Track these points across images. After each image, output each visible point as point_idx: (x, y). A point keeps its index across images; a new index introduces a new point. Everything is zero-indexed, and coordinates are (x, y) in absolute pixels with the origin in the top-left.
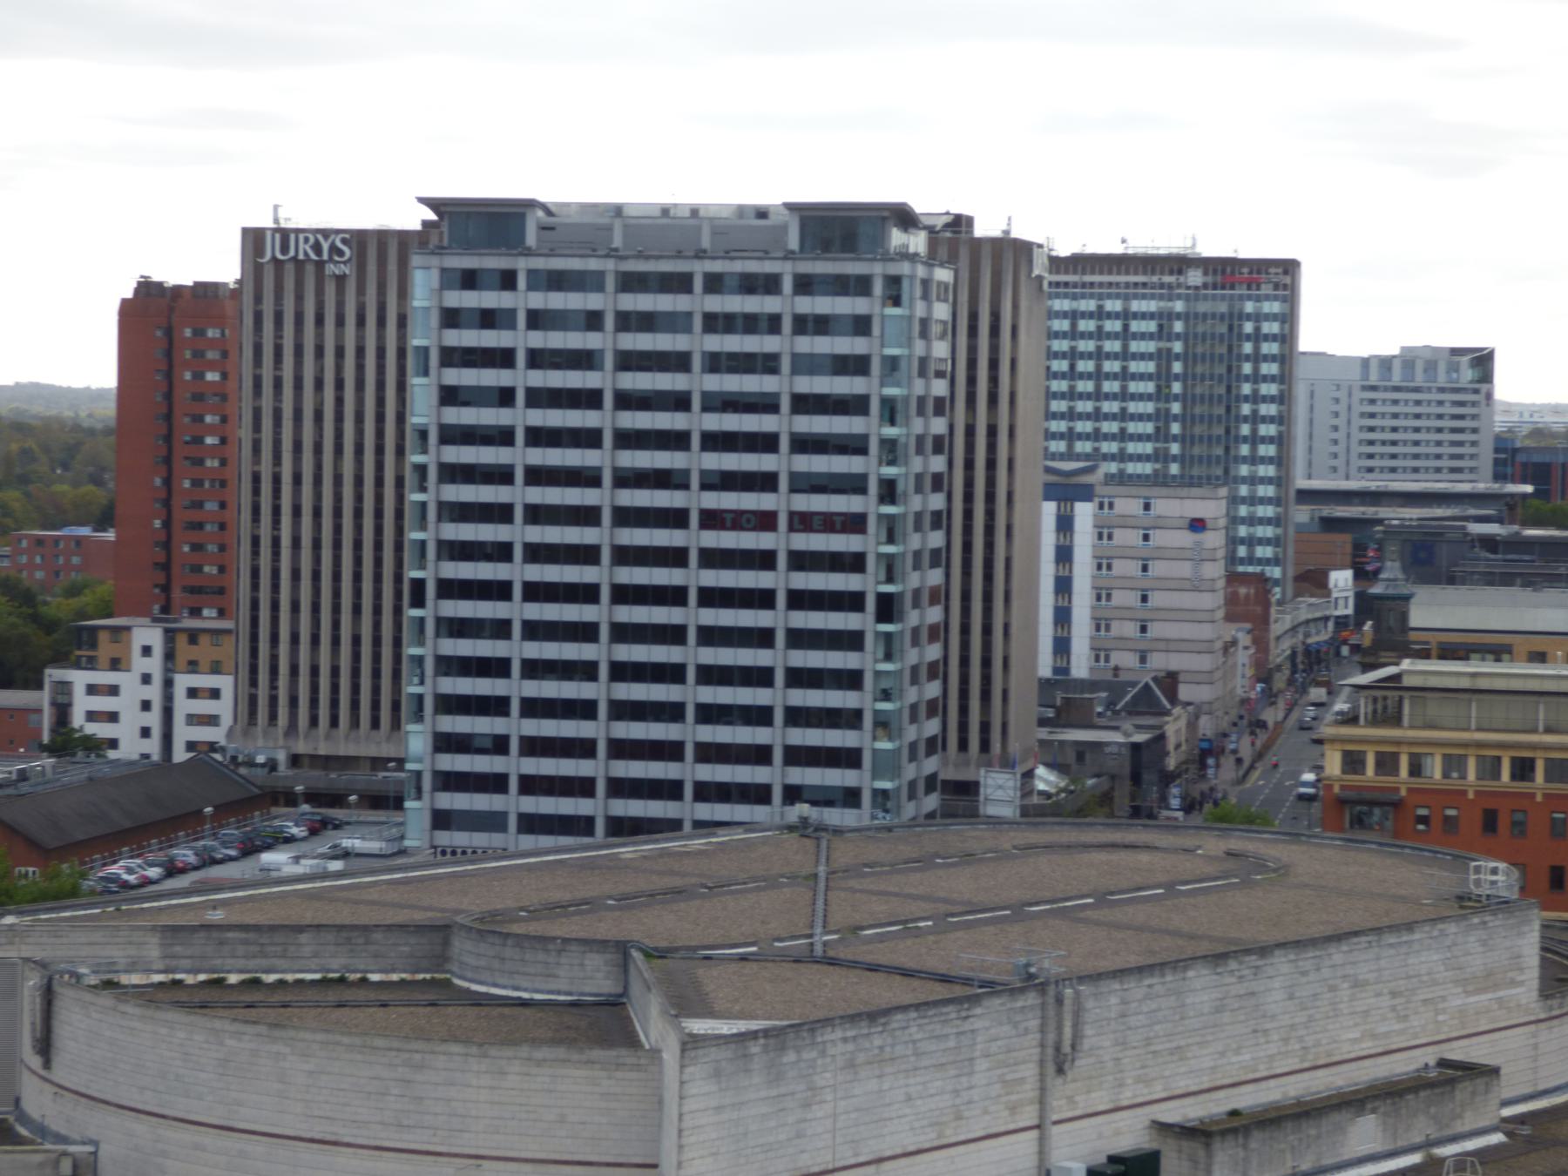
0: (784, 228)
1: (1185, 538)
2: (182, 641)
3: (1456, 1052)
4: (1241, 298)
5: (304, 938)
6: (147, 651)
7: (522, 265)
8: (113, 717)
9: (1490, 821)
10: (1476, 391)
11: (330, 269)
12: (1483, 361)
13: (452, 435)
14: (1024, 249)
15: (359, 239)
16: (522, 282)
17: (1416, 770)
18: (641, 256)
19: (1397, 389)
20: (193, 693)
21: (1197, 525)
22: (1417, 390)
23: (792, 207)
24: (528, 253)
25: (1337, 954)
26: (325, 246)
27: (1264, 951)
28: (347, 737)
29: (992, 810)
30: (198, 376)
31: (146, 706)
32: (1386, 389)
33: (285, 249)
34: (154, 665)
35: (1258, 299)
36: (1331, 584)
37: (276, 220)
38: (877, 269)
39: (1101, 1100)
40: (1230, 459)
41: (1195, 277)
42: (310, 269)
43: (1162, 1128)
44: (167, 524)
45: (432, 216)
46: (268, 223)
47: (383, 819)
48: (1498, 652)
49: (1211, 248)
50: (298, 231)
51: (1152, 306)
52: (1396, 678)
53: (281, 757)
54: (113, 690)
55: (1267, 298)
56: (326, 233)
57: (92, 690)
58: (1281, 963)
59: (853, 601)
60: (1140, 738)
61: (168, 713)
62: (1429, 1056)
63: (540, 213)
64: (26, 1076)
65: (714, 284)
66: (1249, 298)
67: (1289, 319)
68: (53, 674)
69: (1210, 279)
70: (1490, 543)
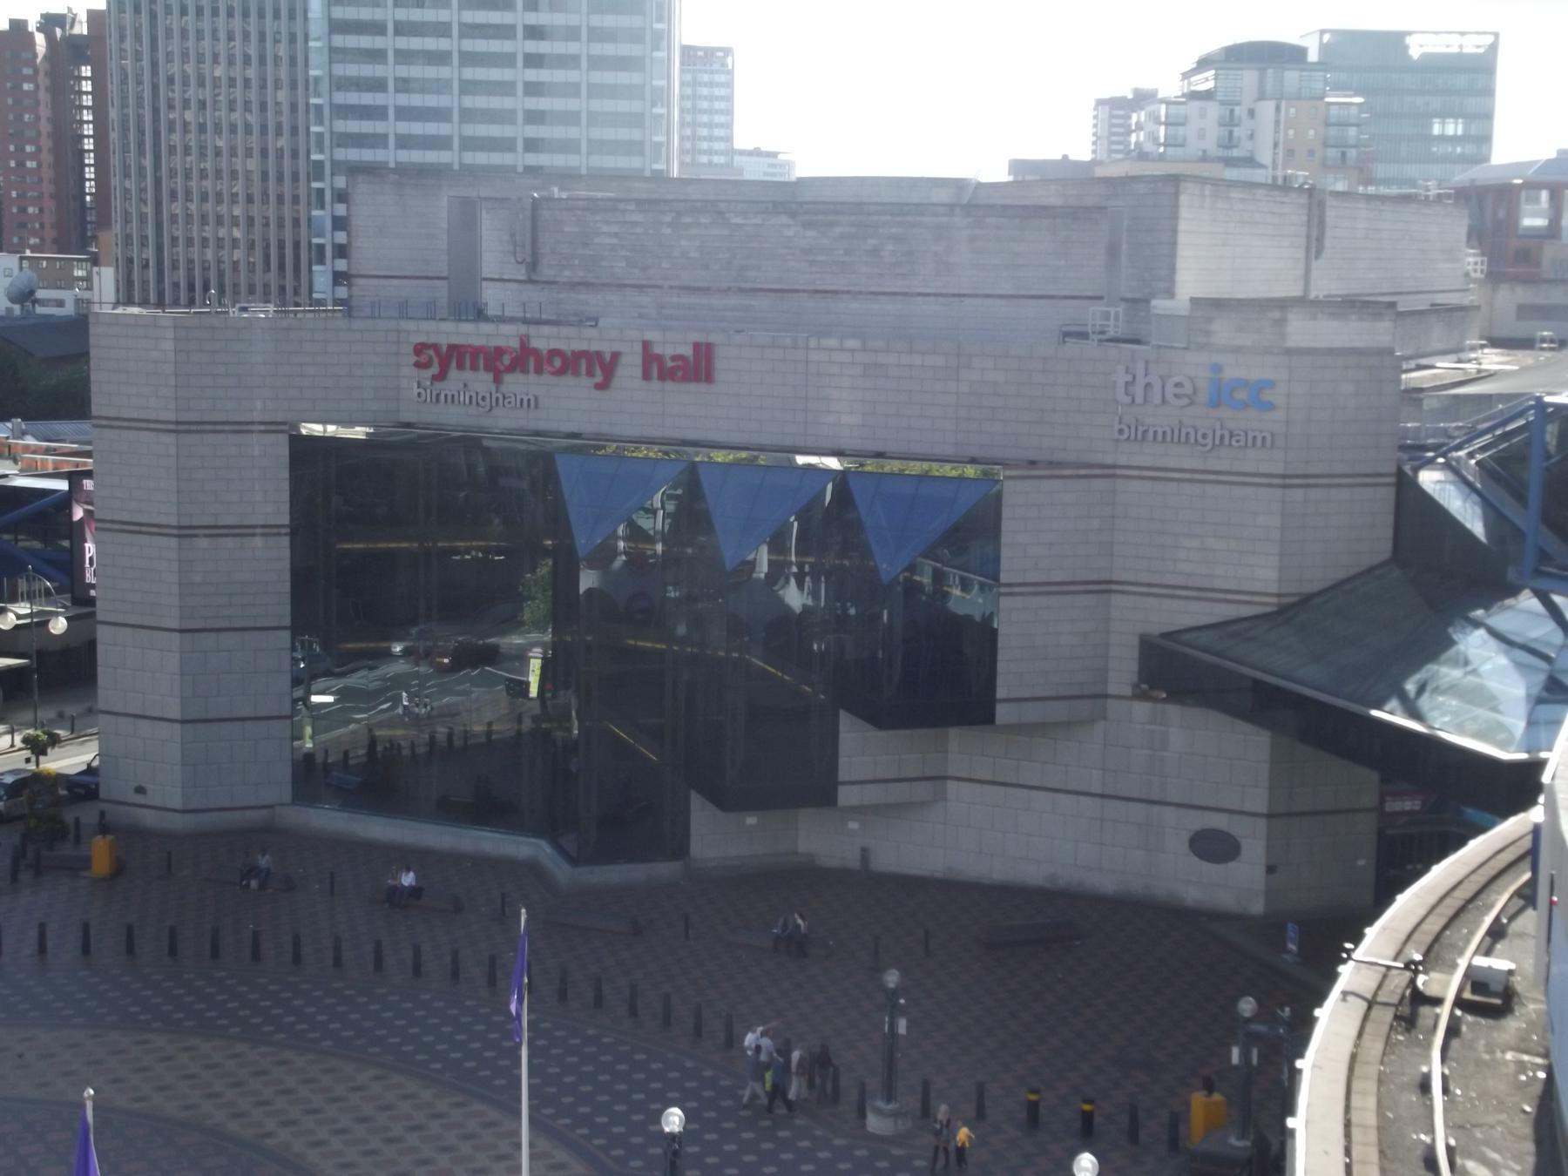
35: (712, 72)
55: (718, 72)
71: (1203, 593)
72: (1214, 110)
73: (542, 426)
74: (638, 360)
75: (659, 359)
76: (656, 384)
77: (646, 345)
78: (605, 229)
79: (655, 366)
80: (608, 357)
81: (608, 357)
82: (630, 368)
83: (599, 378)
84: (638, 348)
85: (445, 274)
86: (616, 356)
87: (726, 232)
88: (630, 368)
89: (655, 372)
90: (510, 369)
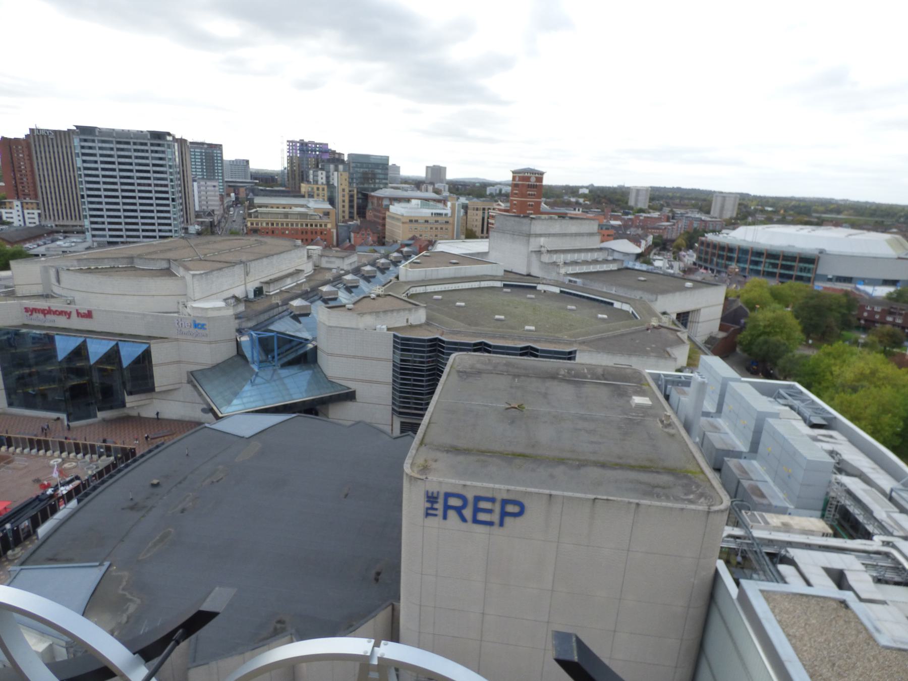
1: (213, 188)
2: (24, 204)
3: (298, 268)
7: (96, 138)
9: (273, 232)
12: (247, 162)
13: (85, 169)
14: (185, 141)
15: (55, 132)
16: (96, 142)
17: (261, 225)
18: (119, 138)
24: (96, 136)
25: (282, 255)
26: (48, 133)
27: (273, 255)
29: (191, 232)
30: (18, 155)
33: (39, 132)
34: (19, 208)
38: (165, 143)
39: (253, 279)
40: (214, 176)
41: (206, 146)
43: (262, 283)
44: (16, 182)
45: (75, 128)
48: (267, 207)
49: (208, 141)
51: (199, 150)
52: (257, 211)
53: (53, 225)
54: (11, 213)
56: (48, 130)
57: (6, 213)
58: (275, 257)
59: (167, 199)
62: (294, 269)
64: (53, 286)
65: (135, 144)
67: (222, 153)
70: (262, 190)
71: (197, 364)
72: (324, 173)
76: (80, 318)
77: (77, 310)
79: (78, 314)
82: (74, 314)
86: (71, 312)
88: (74, 314)
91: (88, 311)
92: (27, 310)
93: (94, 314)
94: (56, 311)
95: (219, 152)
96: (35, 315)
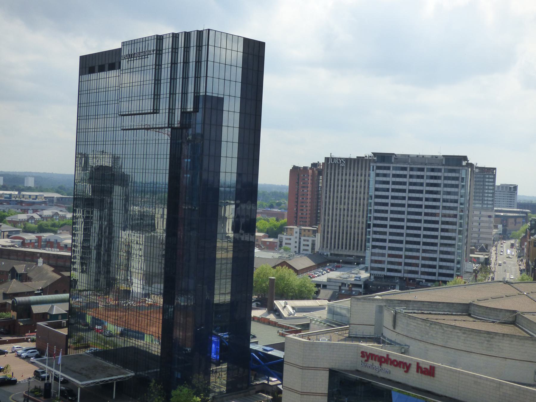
0: (442, 160)
1: (488, 219)
4: (486, 174)
5: (440, 305)
6: (296, 233)
8: (290, 244)
10: (514, 192)
11: (341, 165)
12: (515, 188)
13: (377, 197)
15: (346, 160)
19: (500, 191)
20: (304, 240)
21: (490, 217)
22: (504, 192)
23: (443, 156)
24: (392, 163)
28: (341, 251)
31: (296, 242)
32: (498, 191)
33: (333, 161)
35: (489, 175)
36: (498, 227)
37: (331, 156)
42: (337, 165)
44: (297, 210)
46: (329, 156)
47: (350, 266)
50: (335, 158)
53: (329, 254)
54: (290, 239)
55: (491, 175)
56: (340, 158)
57: (286, 239)
60: (486, 257)
61: (300, 243)
63: (395, 156)
66: (487, 175)
68: (279, 236)
69: (480, 171)
73: (391, 378)
74: (416, 367)
75: (421, 368)
76: (420, 374)
77: (418, 364)
78: (413, 324)
80: (408, 364)
81: (408, 364)
82: (413, 368)
83: (405, 369)
84: (416, 364)
85: (374, 324)
86: (410, 365)
87: (443, 331)
88: (413, 368)
89: (420, 370)
90: (384, 362)
91: (431, 367)
92: (363, 354)
93: (437, 372)
94: (395, 360)
95: (491, 176)
96: (370, 362)
